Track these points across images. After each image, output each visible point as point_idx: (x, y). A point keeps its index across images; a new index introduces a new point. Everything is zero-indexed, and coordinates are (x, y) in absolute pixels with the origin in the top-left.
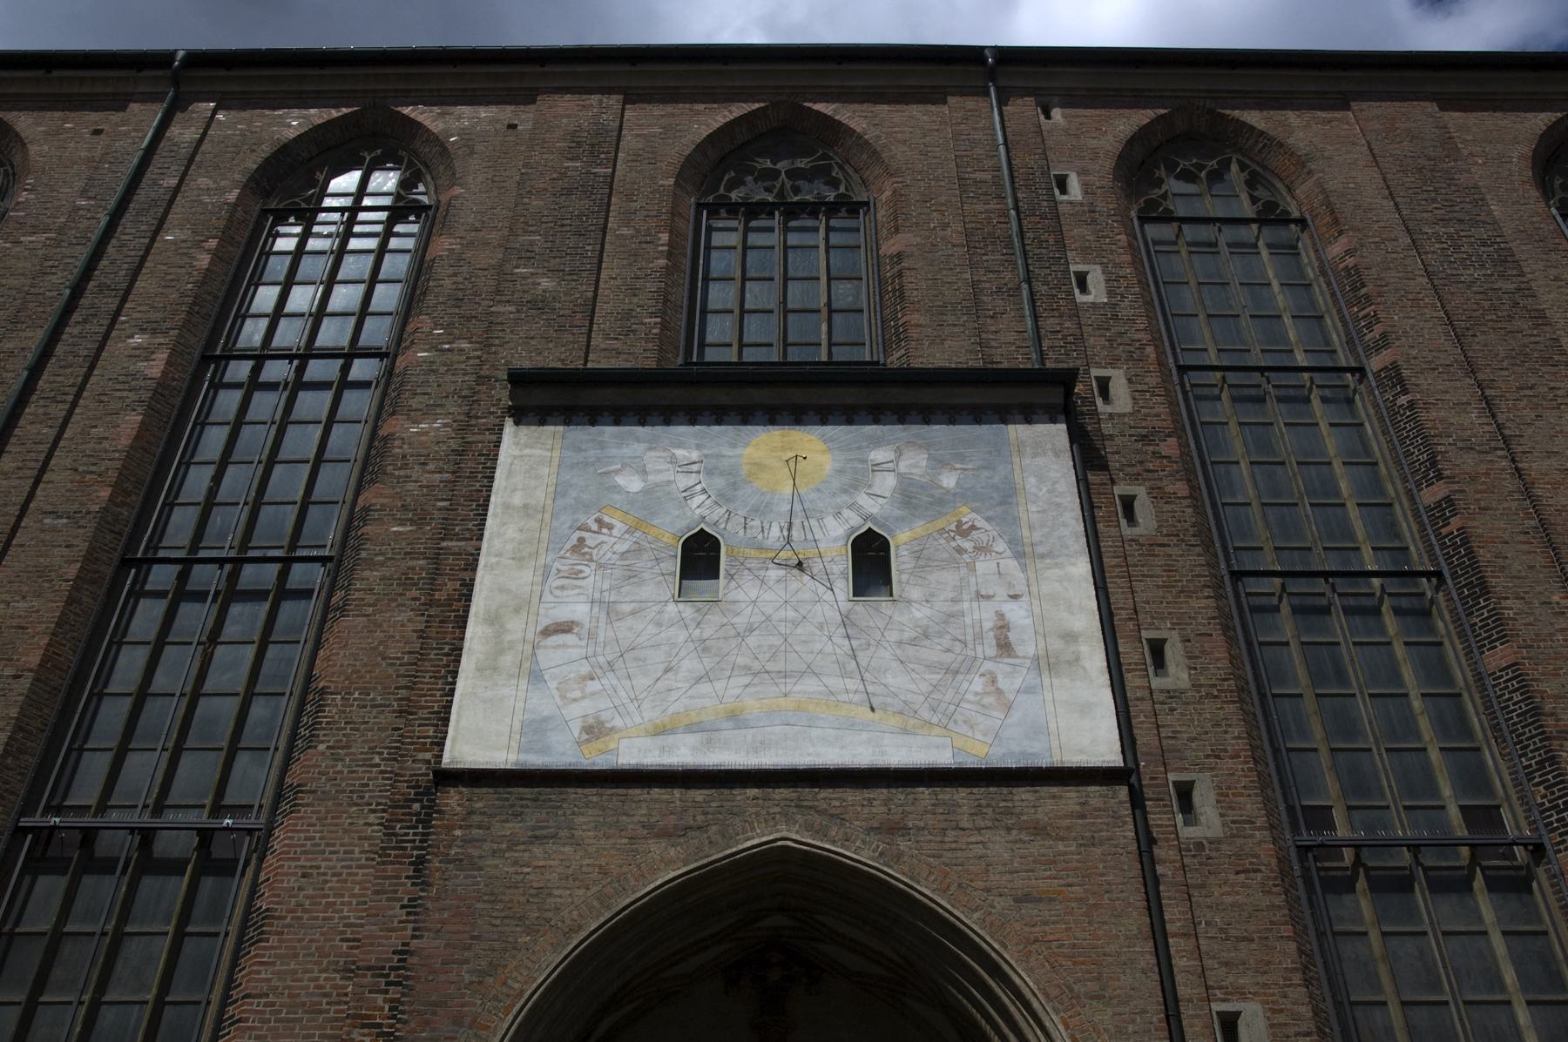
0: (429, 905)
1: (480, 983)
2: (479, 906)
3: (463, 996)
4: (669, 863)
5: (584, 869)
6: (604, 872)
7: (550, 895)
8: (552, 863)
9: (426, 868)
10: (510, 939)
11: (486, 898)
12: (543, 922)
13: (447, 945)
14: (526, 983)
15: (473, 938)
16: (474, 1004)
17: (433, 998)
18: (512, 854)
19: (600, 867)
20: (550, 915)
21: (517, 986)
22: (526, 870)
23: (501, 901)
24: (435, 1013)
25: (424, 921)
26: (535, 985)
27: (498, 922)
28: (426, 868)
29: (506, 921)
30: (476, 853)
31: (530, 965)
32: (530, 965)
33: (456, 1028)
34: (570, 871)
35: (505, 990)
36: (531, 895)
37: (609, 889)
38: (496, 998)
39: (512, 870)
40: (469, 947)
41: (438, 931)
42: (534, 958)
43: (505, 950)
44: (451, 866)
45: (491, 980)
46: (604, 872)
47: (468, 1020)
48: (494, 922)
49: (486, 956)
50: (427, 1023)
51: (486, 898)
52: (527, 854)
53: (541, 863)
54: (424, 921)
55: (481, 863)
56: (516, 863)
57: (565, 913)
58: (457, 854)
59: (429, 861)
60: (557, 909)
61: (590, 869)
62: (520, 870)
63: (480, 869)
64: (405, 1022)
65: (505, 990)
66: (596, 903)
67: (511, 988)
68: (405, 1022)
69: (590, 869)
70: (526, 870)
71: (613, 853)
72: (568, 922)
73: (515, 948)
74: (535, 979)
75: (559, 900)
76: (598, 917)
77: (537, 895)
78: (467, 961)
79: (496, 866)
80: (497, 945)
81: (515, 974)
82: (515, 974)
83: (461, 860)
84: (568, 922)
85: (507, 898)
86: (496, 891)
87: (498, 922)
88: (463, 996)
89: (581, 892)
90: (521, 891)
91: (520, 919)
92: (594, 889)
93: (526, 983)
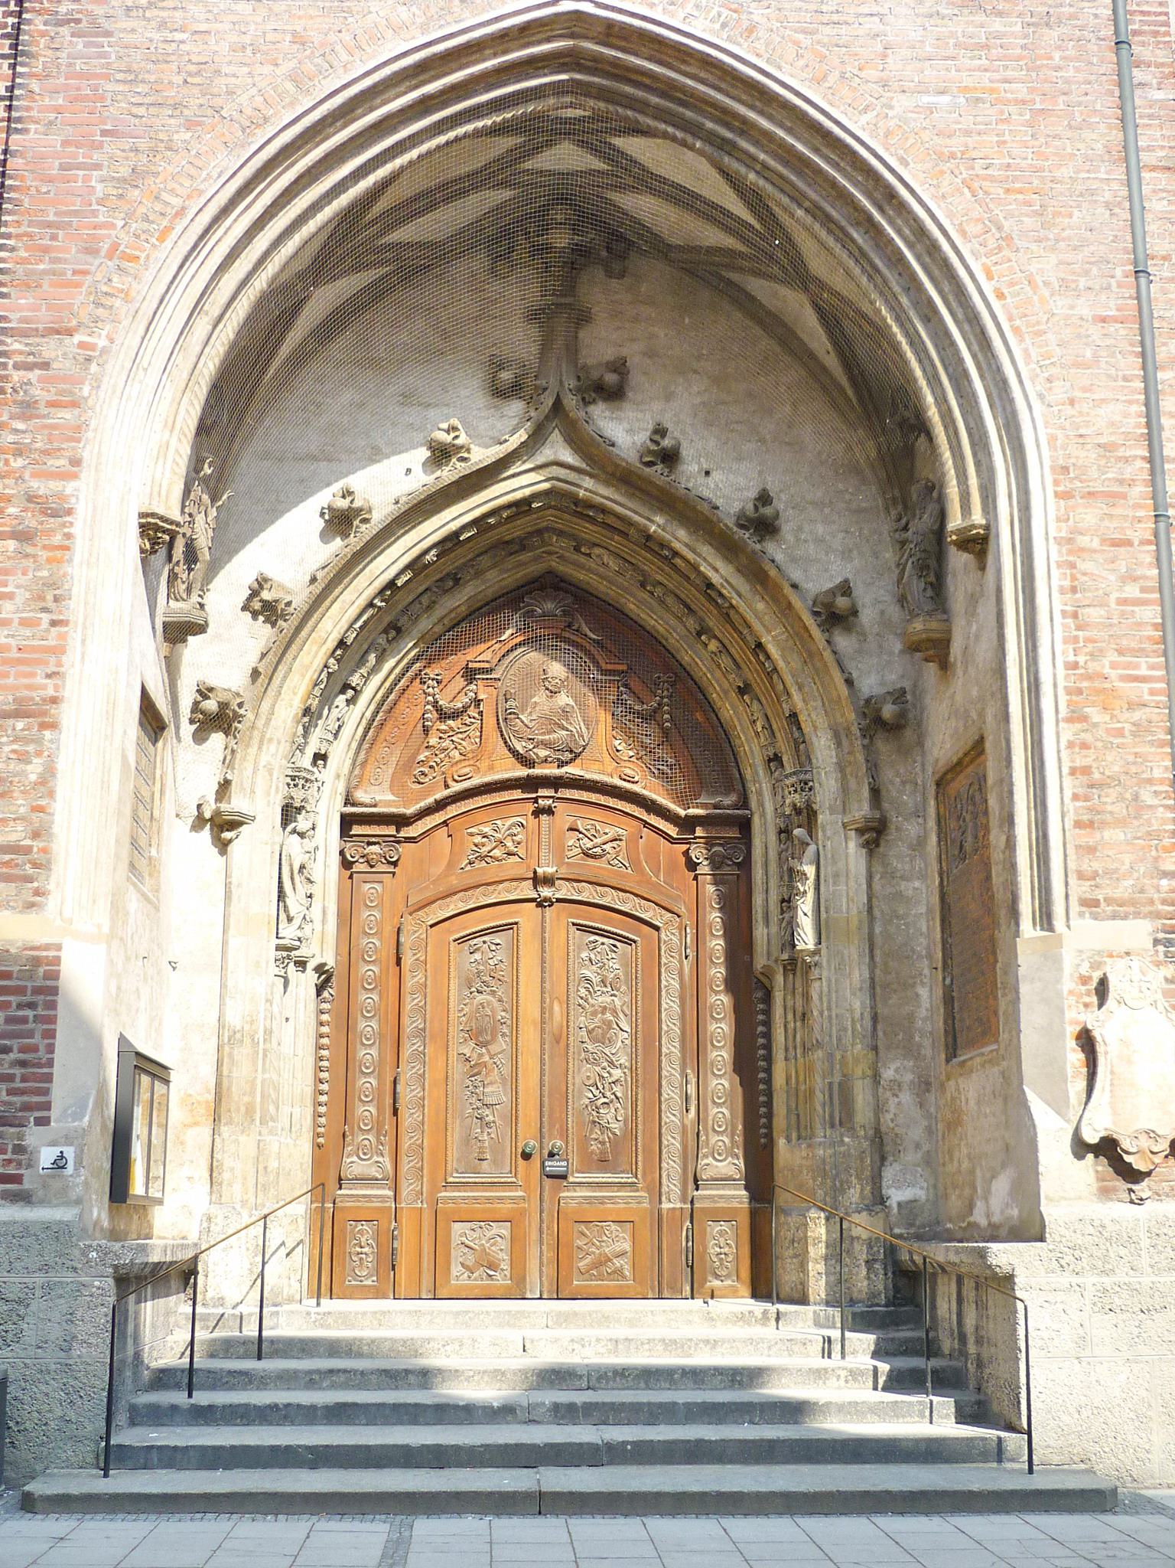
0: (35, 86)
1: (121, 196)
2: (110, 87)
3: (95, 213)
4: (397, 30)
5: (270, 37)
6: (299, 40)
7: (218, 72)
8: (219, 26)
9: (26, 33)
10: (161, 136)
11: (120, 76)
12: (210, 112)
13: (66, 143)
14: (189, 197)
15: (104, 133)
16: (113, 226)
17: (51, 218)
18: (156, 12)
19: (294, 33)
20: (217, 102)
21: (176, 201)
22: (178, 36)
23: (143, 81)
24: (54, 238)
25: (28, 109)
26: (203, 200)
27: (141, 111)
28: (26, 33)
29: (152, 110)
30: (99, 10)
31: (193, 171)
32: (193, 171)
33: (89, 258)
34: (247, 39)
35: (158, 207)
36: (190, 74)
37: (308, 67)
38: (146, 218)
39: (156, 36)
40: (100, 146)
41: (51, 123)
42: (200, 164)
43: (155, 151)
44: (65, 31)
45: (137, 192)
46: (299, 40)
47: (105, 247)
48: (135, 110)
49: (127, 159)
50: (46, 250)
51: (120, 76)
52: (178, 14)
53: (203, 27)
54: (28, 109)
55: (107, 25)
56: (162, 25)
57: (243, 99)
58: (70, 12)
59: (29, 22)
60: (230, 93)
61: (278, 36)
62: (170, 37)
63: (108, 34)
64: (13, 249)
65: (158, 207)
66: (289, 86)
67: (167, 204)
68: (13, 249)
69: (278, 36)
70: (178, 36)
71: (311, 12)
72: (248, 111)
73: (170, 149)
74: (201, 193)
75: (233, 80)
76: (292, 104)
77: (198, 73)
78: (97, 167)
79: (133, 30)
80: (143, 144)
81: (171, 185)
82: (171, 185)
83: (78, 21)
84: (248, 111)
85: (153, 78)
86: (135, 67)
87: (141, 111)
88: (95, 213)
89: (267, 69)
90: (174, 66)
91: (175, 107)
92: (287, 66)
93: (189, 197)
